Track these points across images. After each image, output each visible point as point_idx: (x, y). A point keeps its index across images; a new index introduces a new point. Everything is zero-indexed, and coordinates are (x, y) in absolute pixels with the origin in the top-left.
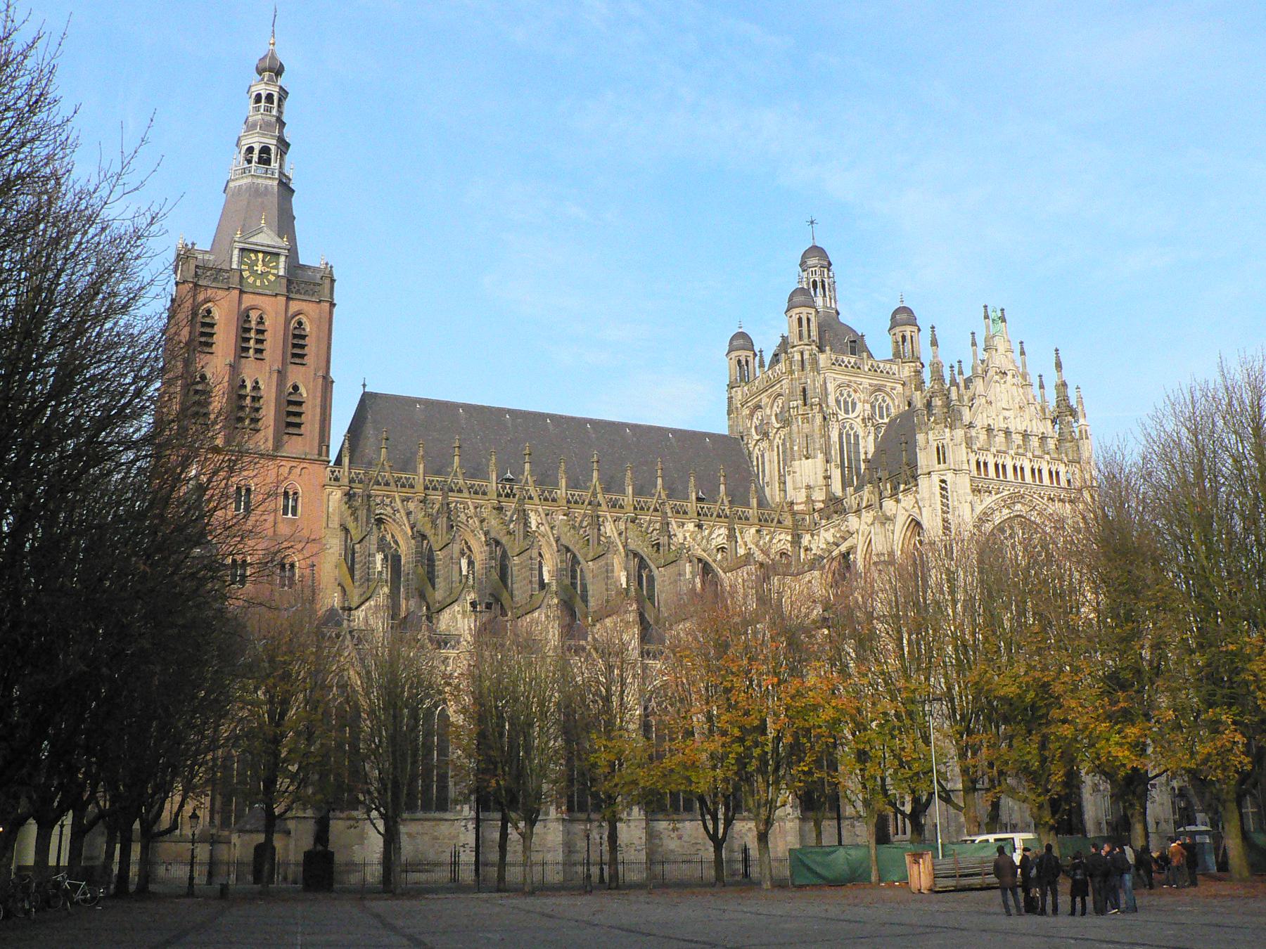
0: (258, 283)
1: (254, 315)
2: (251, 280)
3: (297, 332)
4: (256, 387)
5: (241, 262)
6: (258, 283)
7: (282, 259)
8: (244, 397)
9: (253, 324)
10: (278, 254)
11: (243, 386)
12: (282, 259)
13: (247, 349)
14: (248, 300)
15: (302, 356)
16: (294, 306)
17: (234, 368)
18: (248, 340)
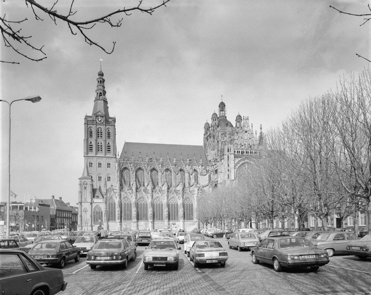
0: (100, 123)
1: (100, 129)
2: (98, 122)
3: (108, 132)
4: (101, 144)
5: (96, 119)
6: (100, 123)
7: (104, 117)
8: (99, 146)
9: (100, 131)
10: (103, 116)
11: (99, 144)
12: (104, 117)
13: (99, 136)
14: (98, 126)
15: (110, 137)
16: (107, 127)
17: (96, 140)
18: (99, 134)
